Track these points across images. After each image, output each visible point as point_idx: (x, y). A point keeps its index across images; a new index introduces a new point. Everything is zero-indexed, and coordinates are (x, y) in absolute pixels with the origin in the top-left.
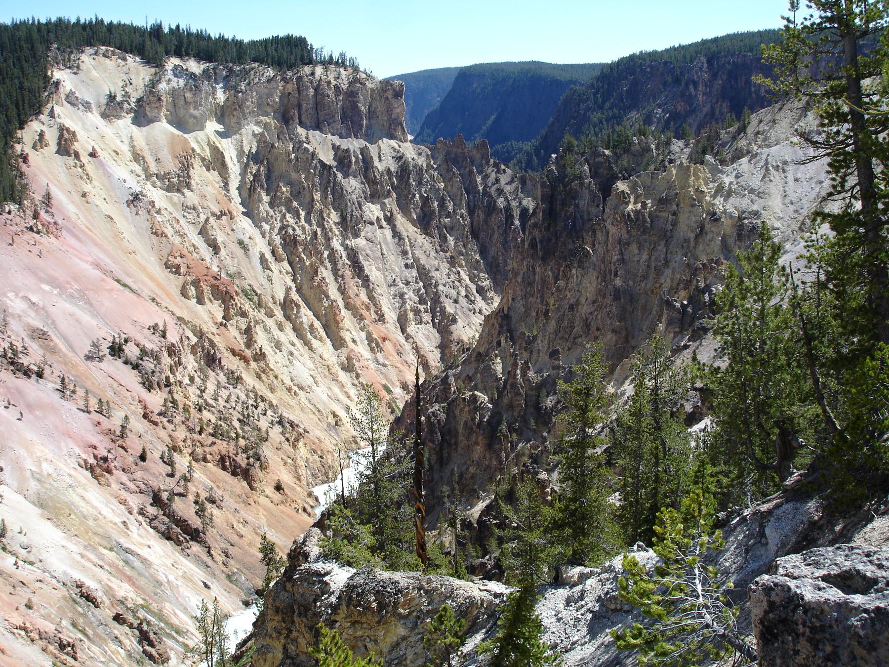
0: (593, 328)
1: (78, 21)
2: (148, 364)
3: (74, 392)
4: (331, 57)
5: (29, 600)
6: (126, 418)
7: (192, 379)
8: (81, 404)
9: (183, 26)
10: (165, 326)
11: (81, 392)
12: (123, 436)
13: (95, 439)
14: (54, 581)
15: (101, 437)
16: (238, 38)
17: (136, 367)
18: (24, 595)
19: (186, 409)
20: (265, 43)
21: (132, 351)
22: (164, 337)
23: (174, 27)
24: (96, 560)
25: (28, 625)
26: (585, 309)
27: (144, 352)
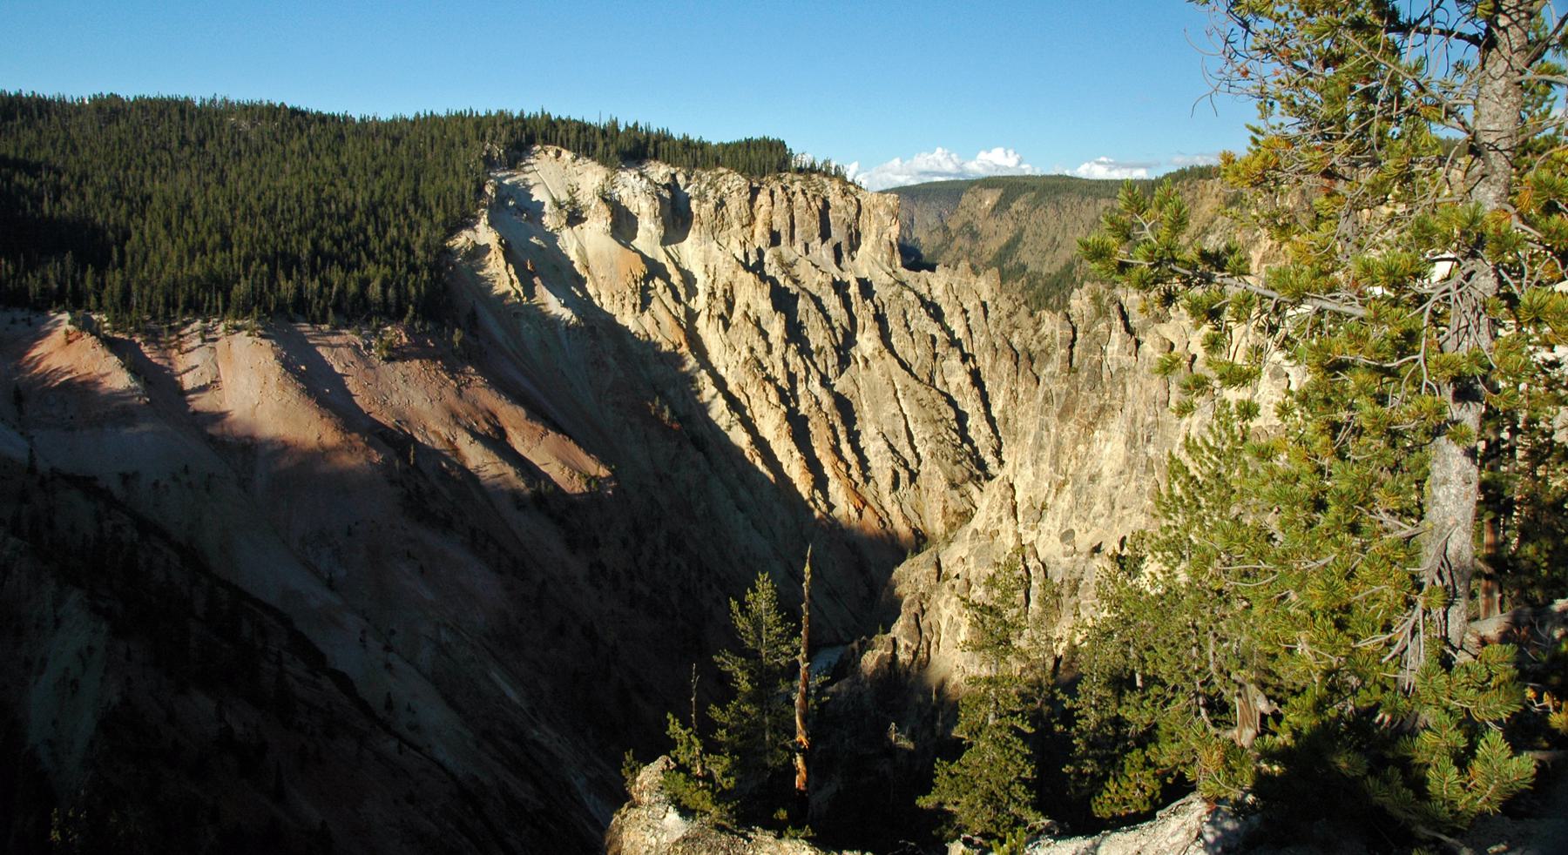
0: (1117, 507)
1: (522, 113)
4: (813, 165)
7: (625, 543)
9: (642, 125)
16: (705, 140)
20: (738, 145)
23: (631, 125)
26: (1107, 482)
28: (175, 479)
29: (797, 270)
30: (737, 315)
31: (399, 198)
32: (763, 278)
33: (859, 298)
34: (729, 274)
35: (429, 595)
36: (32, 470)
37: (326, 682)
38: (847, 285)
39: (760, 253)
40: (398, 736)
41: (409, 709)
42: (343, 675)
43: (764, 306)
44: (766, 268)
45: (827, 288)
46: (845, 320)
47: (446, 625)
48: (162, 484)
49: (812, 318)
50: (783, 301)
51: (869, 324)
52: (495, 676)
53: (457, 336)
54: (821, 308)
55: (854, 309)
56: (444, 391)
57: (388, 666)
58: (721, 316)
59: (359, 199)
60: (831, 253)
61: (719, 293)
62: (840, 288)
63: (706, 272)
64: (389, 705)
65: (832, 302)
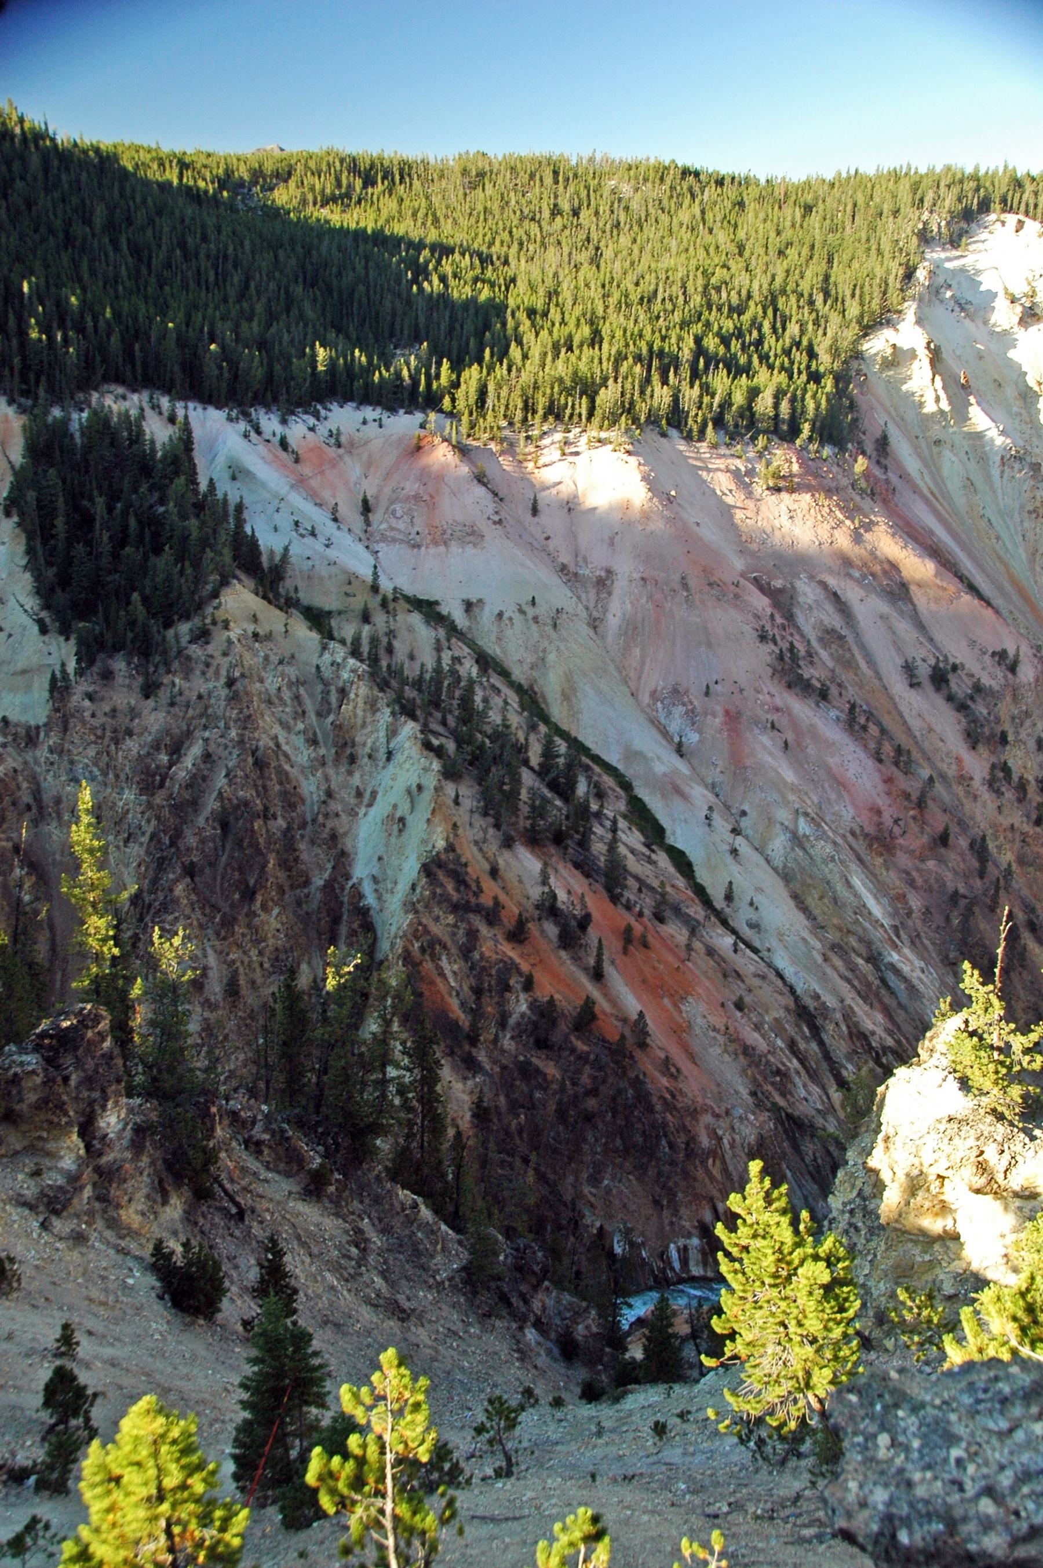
2: (981, 709)
3: (864, 728)
5: (741, 998)
6: (931, 779)
8: (872, 745)
10: (1017, 655)
11: (873, 730)
12: (921, 804)
13: (882, 802)
14: (779, 983)
15: (888, 802)
17: (962, 707)
18: (737, 989)
19: (1022, 787)
21: (959, 686)
22: (1013, 669)
24: (842, 969)
25: (731, 1030)
27: (978, 688)
28: (521, 611)
31: (805, 286)
35: (789, 776)
36: (375, 589)
37: (662, 859)
40: (734, 932)
41: (751, 904)
42: (682, 853)
47: (806, 814)
48: (506, 615)
52: (857, 882)
53: (861, 464)
56: (837, 533)
57: (734, 852)
59: (756, 286)
64: (729, 897)
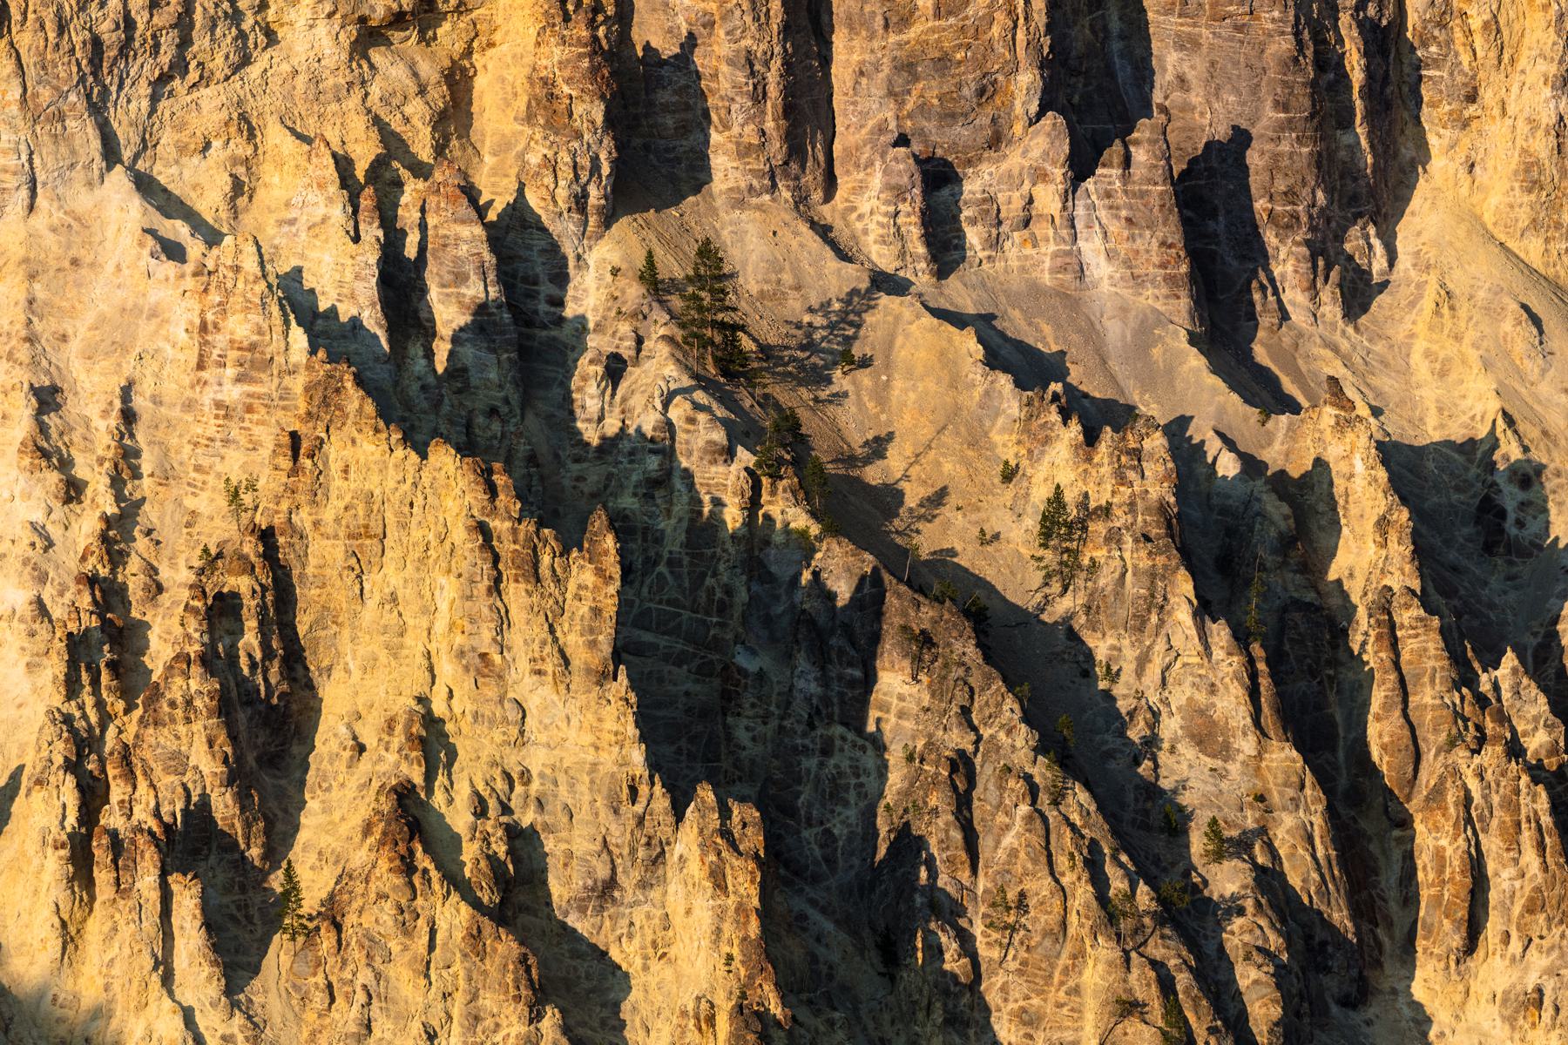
29: (851, 411)
30: (334, 829)
32: (553, 483)
33: (1423, 645)
34: (254, 456)
38: (1309, 502)
39: (524, 258)
43: (571, 741)
44: (588, 393)
45: (1121, 561)
46: (1299, 836)
49: (1008, 834)
50: (741, 667)
51: (1516, 873)
54: (1085, 737)
55: (1380, 733)
58: (189, 842)
60: (1159, 243)
61: (168, 634)
62: (1244, 549)
63: (47, 452)
65: (1183, 681)
